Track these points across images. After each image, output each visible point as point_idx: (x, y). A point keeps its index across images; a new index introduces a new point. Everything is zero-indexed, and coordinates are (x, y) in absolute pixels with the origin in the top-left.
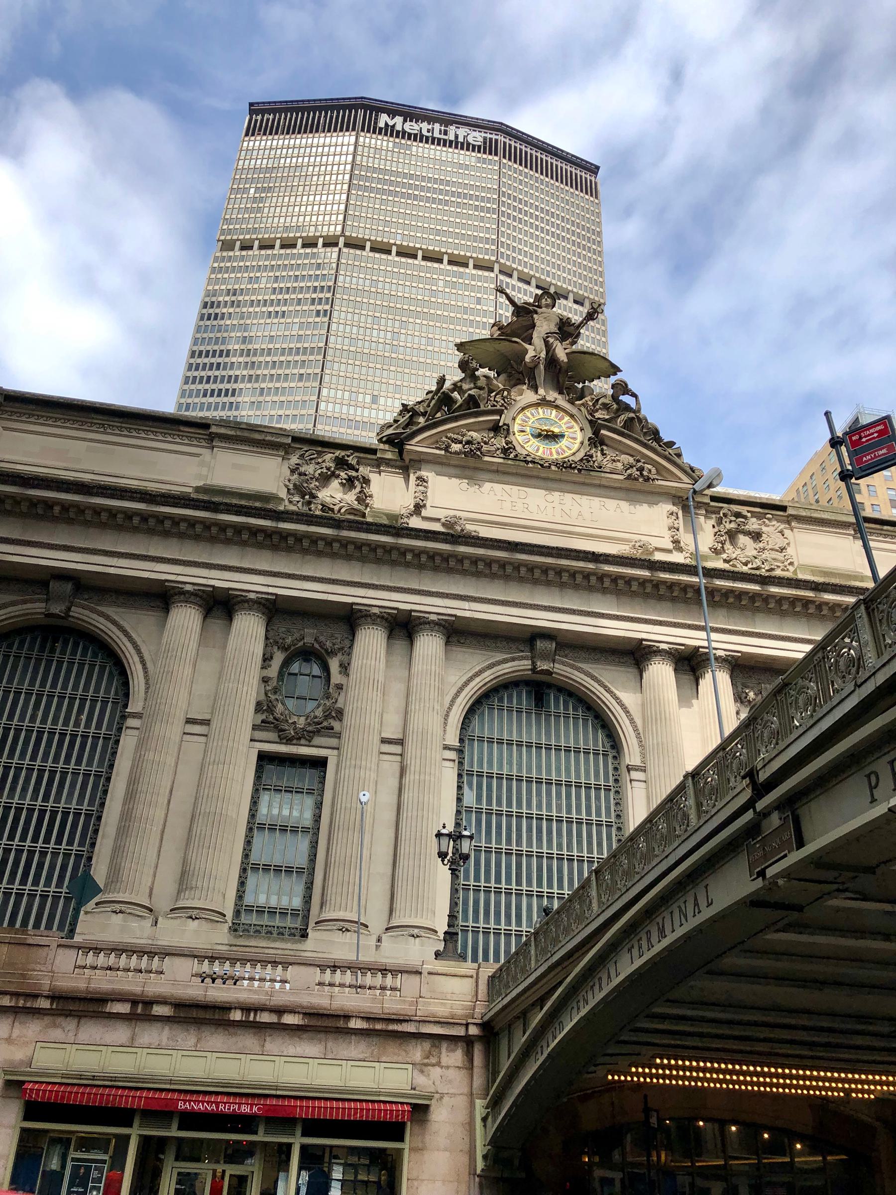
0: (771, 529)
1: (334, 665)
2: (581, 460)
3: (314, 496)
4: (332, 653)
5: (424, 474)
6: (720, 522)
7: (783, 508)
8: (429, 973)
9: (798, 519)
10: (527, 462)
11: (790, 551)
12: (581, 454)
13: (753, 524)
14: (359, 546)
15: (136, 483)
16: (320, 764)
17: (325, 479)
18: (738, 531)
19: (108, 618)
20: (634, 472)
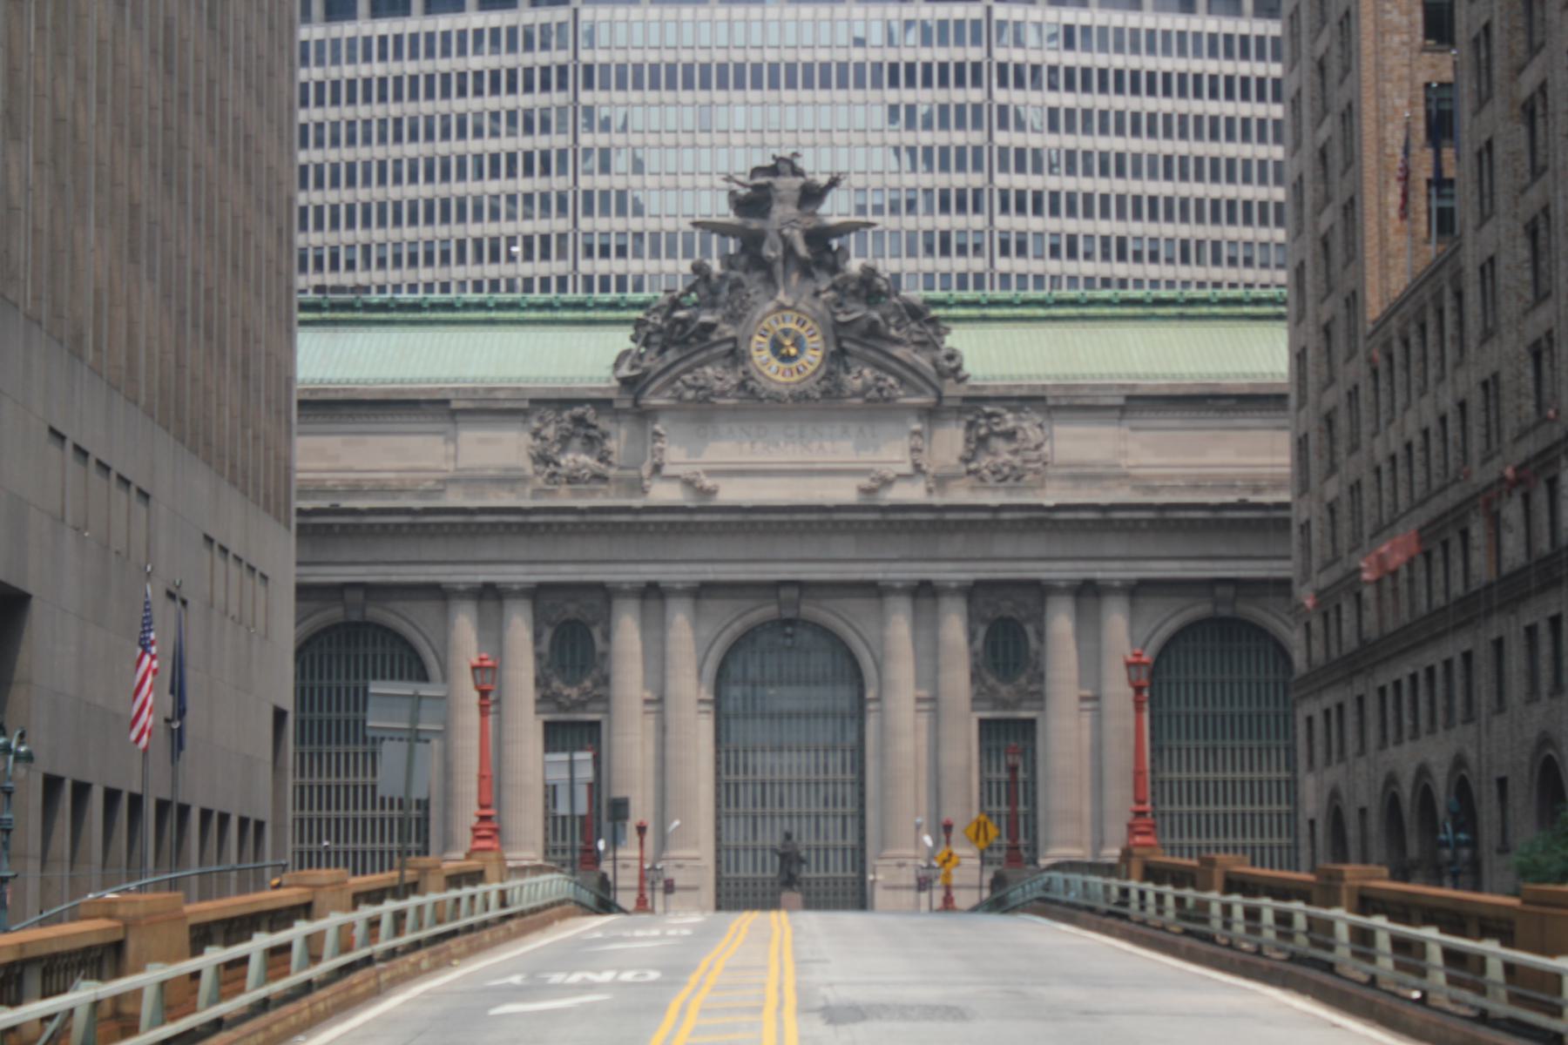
0: (1029, 426)
1: (596, 633)
2: (824, 378)
3: (557, 464)
4: (595, 623)
5: (658, 427)
6: (971, 425)
7: (1043, 398)
8: (695, 888)
9: (1057, 408)
10: (761, 400)
11: (1046, 449)
12: (822, 372)
13: (1010, 421)
14: (604, 524)
15: (392, 475)
16: (596, 725)
17: (565, 441)
18: (992, 433)
19: (397, 614)
20: (873, 393)
